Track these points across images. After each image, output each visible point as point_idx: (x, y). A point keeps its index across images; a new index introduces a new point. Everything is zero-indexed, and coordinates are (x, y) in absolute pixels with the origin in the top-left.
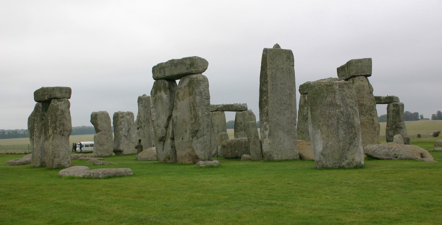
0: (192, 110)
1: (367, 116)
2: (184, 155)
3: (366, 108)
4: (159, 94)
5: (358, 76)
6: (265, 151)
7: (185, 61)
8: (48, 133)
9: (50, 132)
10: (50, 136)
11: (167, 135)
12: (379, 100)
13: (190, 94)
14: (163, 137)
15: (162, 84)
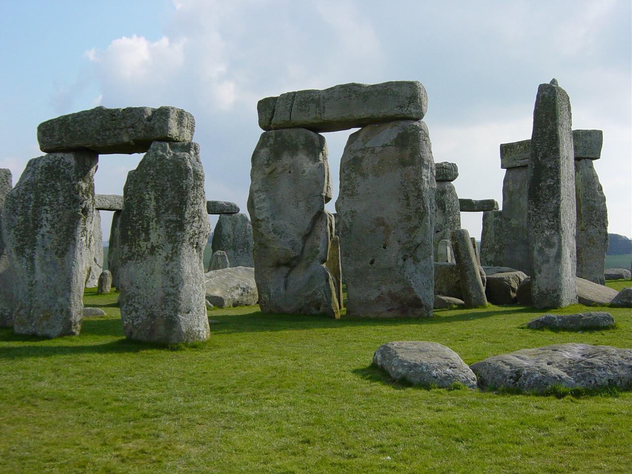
0: (412, 199)
1: (599, 228)
2: (373, 298)
3: (598, 213)
4: (286, 159)
5: (584, 158)
6: (543, 289)
7: (396, 89)
8: (147, 239)
9: (157, 235)
10: (153, 250)
11: (306, 254)
12: (468, 205)
13: (404, 164)
14: (295, 258)
15: (302, 138)
